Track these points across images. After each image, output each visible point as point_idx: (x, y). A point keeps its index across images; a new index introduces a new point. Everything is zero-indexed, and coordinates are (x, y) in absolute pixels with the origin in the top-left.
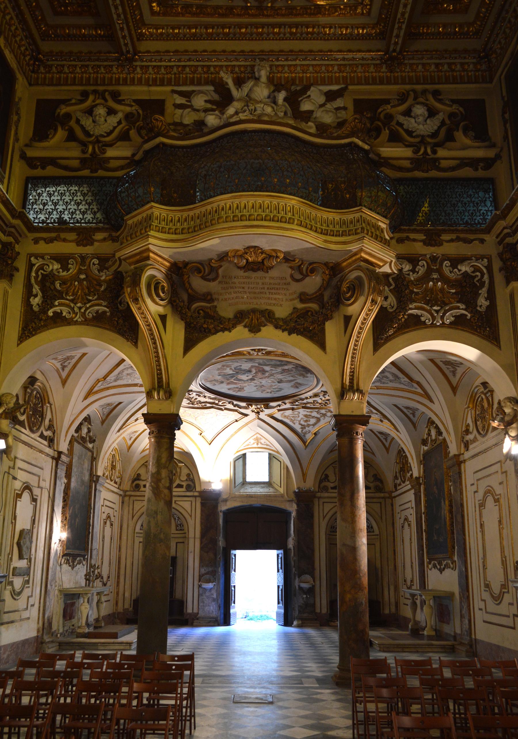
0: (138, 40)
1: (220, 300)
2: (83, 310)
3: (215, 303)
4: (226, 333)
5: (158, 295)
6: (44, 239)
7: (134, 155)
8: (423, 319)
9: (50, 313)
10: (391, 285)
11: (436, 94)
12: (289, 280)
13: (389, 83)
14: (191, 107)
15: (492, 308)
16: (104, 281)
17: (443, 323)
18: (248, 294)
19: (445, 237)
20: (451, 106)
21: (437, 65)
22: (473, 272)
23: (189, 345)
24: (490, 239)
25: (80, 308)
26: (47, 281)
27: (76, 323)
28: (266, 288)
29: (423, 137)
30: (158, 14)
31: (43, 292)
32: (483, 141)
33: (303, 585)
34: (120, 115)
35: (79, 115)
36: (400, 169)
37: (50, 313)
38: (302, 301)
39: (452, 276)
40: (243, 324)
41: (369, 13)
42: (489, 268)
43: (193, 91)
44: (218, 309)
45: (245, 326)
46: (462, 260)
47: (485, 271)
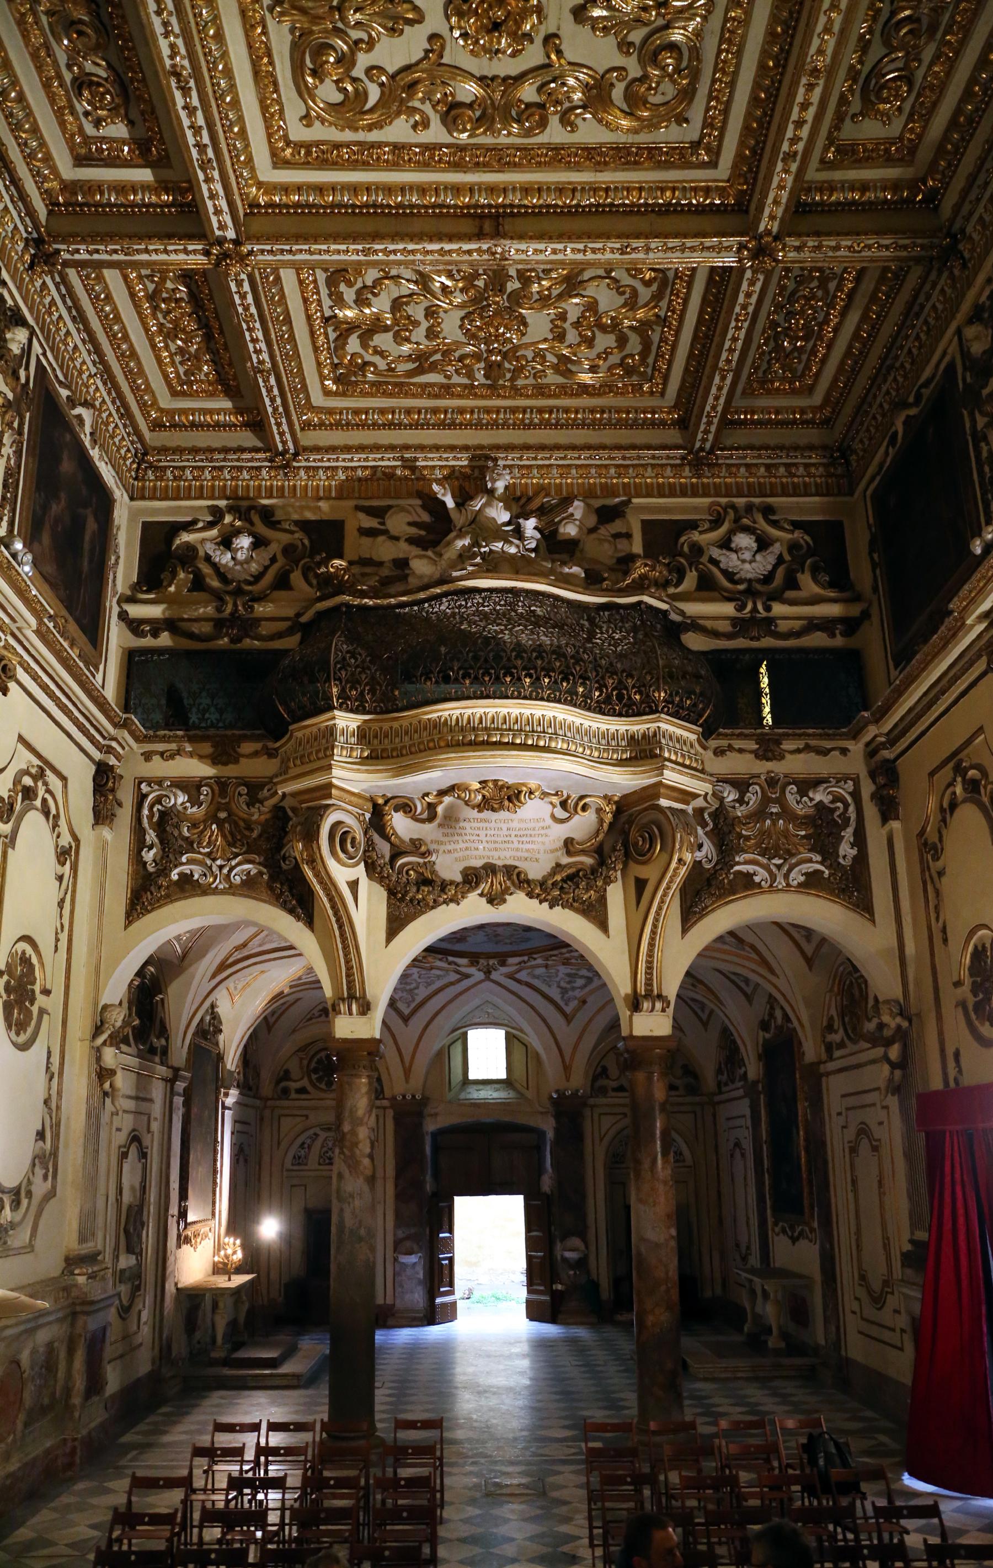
0: (302, 429)
2: (225, 871)
4: (452, 905)
5: (344, 850)
6: (162, 754)
7: (298, 615)
8: (757, 879)
9: (174, 876)
11: (767, 511)
12: (549, 821)
13: (695, 494)
14: (385, 532)
15: (862, 859)
16: (256, 822)
17: (788, 885)
19: (787, 745)
20: (792, 532)
21: (768, 467)
22: (832, 802)
23: (395, 926)
24: (857, 748)
25: (221, 867)
26: (165, 821)
27: (216, 892)
29: (750, 581)
30: (336, 394)
31: (161, 842)
33: (568, 1254)
34: (274, 548)
35: (210, 548)
36: (715, 634)
37: (174, 876)
38: (569, 853)
39: (800, 810)
41: (662, 394)
42: (856, 795)
43: (390, 507)
44: (437, 867)
45: (481, 895)
46: (816, 783)
47: (849, 799)
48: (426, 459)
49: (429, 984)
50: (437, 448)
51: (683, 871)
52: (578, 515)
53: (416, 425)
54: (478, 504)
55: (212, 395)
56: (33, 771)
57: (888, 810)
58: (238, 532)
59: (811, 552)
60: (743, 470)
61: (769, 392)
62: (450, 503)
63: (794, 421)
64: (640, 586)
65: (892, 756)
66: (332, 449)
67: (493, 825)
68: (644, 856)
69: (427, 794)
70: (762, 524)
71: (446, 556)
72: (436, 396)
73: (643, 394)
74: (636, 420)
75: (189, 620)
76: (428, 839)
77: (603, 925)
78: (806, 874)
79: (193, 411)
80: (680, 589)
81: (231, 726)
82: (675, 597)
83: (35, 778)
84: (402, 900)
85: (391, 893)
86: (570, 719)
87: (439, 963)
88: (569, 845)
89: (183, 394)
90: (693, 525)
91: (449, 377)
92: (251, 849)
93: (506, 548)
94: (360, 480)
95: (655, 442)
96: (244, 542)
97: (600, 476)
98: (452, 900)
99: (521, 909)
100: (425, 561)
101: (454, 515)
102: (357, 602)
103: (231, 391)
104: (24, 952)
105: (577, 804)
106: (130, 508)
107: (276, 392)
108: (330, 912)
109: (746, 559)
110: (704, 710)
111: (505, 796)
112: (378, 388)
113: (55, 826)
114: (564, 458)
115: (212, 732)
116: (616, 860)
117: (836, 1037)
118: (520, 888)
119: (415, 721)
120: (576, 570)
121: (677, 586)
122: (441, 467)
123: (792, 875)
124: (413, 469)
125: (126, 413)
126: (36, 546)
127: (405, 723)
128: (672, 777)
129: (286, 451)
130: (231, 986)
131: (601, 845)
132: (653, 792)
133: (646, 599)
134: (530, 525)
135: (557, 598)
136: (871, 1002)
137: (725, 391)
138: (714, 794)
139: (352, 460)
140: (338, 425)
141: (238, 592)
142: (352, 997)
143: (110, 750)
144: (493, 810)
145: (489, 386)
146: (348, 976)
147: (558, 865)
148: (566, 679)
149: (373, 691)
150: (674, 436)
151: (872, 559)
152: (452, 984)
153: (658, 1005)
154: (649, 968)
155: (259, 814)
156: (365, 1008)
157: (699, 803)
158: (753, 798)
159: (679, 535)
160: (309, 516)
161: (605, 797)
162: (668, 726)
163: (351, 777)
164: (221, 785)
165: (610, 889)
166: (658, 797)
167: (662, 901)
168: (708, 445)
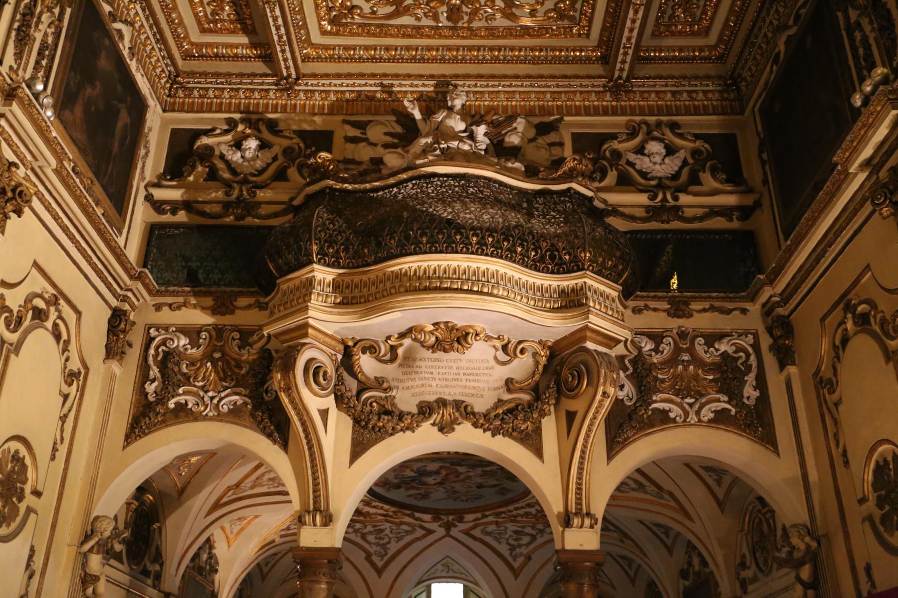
0: (303, 61)
1: (400, 388)
2: (215, 401)
3: (394, 393)
4: (408, 433)
5: (317, 382)
6: (170, 306)
7: (292, 199)
8: (672, 415)
10: (628, 369)
11: (673, 126)
12: (493, 363)
13: (614, 114)
14: (366, 140)
15: (764, 399)
16: (247, 362)
17: (700, 420)
18: (438, 382)
19: (695, 306)
20: (694, 142)
21: (674, 93)
22: (735, 352)
23: (358, 449)
24: (755, 308)
25: (212, 398)
26: (168, 359)
27: (206, 418)
28: (462, 374)
29: (660, 179)
31: (163, 377)
32: (737, 184)
34: (276, 150)
35: (224, 149)
36: (633, 218)
37: (171, 405)
38: (509, 391)
39: (707, 358)
40: (432, 421)
42: (756, 346)
43: (371, 121)
44: (396, 401)
45: (433, 424)
46: (721, 336)
47: (750, 350)
48: (400, 85)
49: (399, 539)
50: (409, 76)
51: (607, 403)
52: (520, 129)
54: (440, 116)
55: (233, 32)
56: (46, 296)
57: (785, 357)
58: (246, 137)
59: (710, 157)
60: (653, 95)
61: (673, 34)
62: (417, 115)
63: (694, 58)
64: (569, 176)
65: (787, 313)
66: (326, 76)
67: (444, 364)
68: (572, 391)
69: (389, 338)
70: (669, 135)
71: (412, 152)
72: (410, 36)
73: (572, 36)
74: (567, 57)
75: (203, 202)
76: (390, 378)
77: (539, 452)
78: (714, 412)
79: (217, 45)
80: (601, 185)
81: (230, 284)
82: (599, 190)
83: (48, 303)
84: (365, 427)
85: (356, 421)
86: (510, 273)
87: (407, 519)
88: (509, 384)
89: (210, 31)
90: (614, 136)
91: (418, 19)
92: (239, 383)
93: (462, 146)
94: (347, 101)
95: (581, 73)
96: (252, 144)
98: (408, 428)
99: (468, 438)
100: (395, 156)
101: (421, 125)
103: (246, 31)
104: (17, 452)
105: (516, 347)
106: (162, 118)
107: (280, 21)
108: (302, 435)
109: (656, 161)
111: (455, 338)
112: (365, 29)
113: (65, 350)
114: (510, 86)
115: (213, 289)
116: (550, 395)
117: (748, 574)
118: (466, 418)
119: (380, 274)
120: (517, 165)
121: (600, 181)
122: (412, 92)
123: (703, 412)
124: (390, 93)
125: (162, 40)
126: (67, 113)
127: (373, 276)
128: (596, 321)
129: (289, 76)
130: (227, 526)
131: (537, 384)
132: (579, 336)
133: (574, 186)
135: (501, 184)
136: (779, 533)
137: (637, 24)
138: (632, 341)
139: (341, 85)
140: (331, 59)
141: (245, 181)
142: (317, 509)
143: (125, 299)
144: (445, 351)
145: (450, 28)
146: (315, 491)
147: (500, 401)
149: (346, 250)
150: (597, 69)
151: (761, 158)
152: (418, 539)
153: (587, 522)
154: (579, 489)
155: (249, 355)
156: (328, 520)
157: (620, 350)
158: (667, 348)
160: (306, 127)
161: (540, 342)
162: (592, 282)
163: (326, 320)
164: (218, 331)
165: (544, 421)
166: (584, 339)
167: (589, 430)
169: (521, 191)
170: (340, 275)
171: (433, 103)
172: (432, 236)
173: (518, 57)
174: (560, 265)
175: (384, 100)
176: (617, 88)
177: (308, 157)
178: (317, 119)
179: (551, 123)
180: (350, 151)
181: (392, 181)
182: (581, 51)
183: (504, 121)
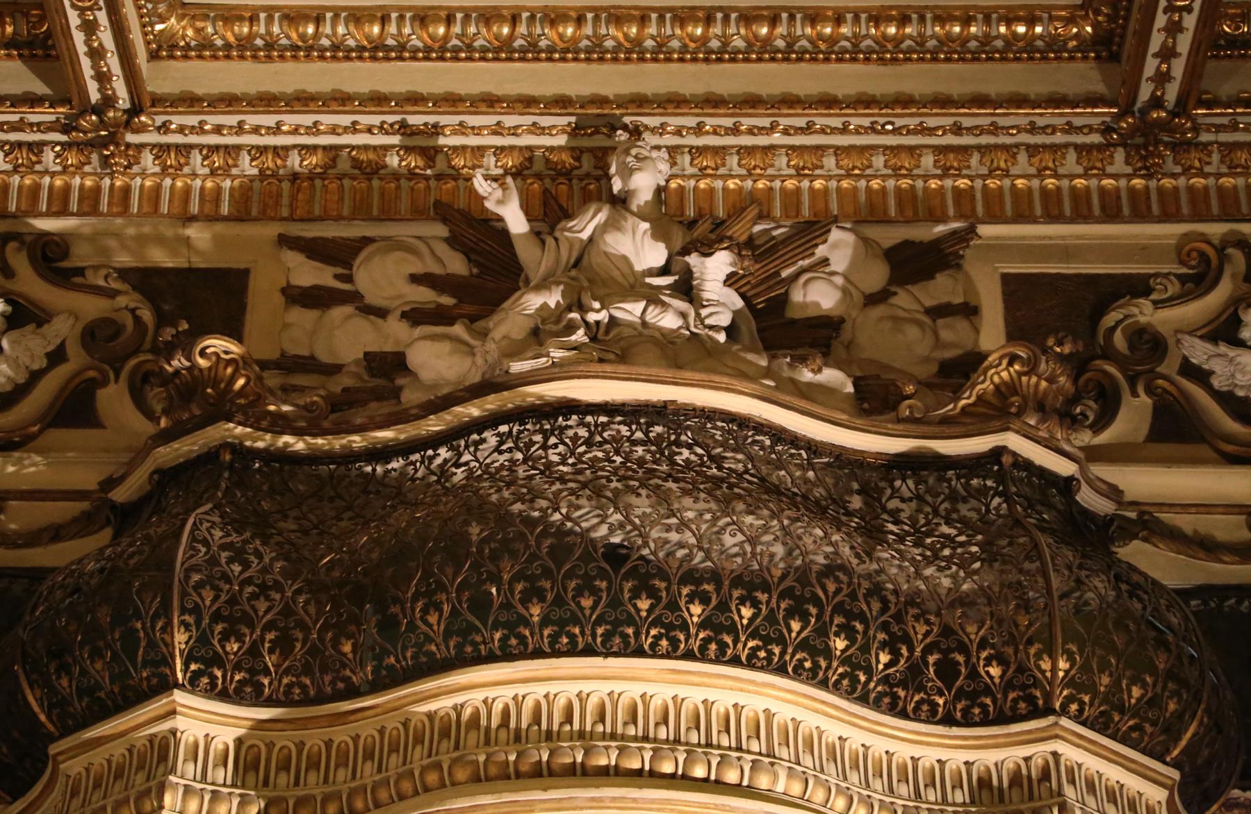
7: (110, 483)
13: (1140, 213)
14: (353, 298)
34: (61, 329)
36: (1206, 547)
43: (367, 241)
48: (462, 129)
50: (489, 102)
53: (438, 52)
54: (586, 225)
62: (516, 221)
64: (998, 411)
66: (229, 102)
71: (497, 334)
74: (986, 40)
80: (1104, 437)
82: (1094, 454)
86: (811, 721)
90: (1138, 287)
93: (653, 315)
94: (295, 177)
95: (1035, 89)
97: (897, 173)
100: (445, 347)
101: (526, 253)
102: (262, 442)
110: (1180, 720)
114: (808, 129)
120: (831, 376)
121: (1097, 427)
122: (500, 151)
124: (430, 154)
127: (367, 729)
129: (109, 101)
133: (1014, 442)
134: (714, 270)
135: (779, 435)
139: (277, 130)
140: (243, 49)
148: (797, 611)
149: (283, 645)
150: (1083, 76)
159: (1100, 310)
160: (160, 258)
168: (1171, 93)
169: (843, 459)
170: (260, 725)
171: (563, 187)
172: (559, 601)
173: (832, 40)
174: (973, 697)
175: (412, 175)
176: (1147, 137)
177: (168, 351)
178: (198, 234)
179: (936, 245)
180: (302, 331)
181: (434, 425)
182: (1031, 22)
183: (786, 240)
